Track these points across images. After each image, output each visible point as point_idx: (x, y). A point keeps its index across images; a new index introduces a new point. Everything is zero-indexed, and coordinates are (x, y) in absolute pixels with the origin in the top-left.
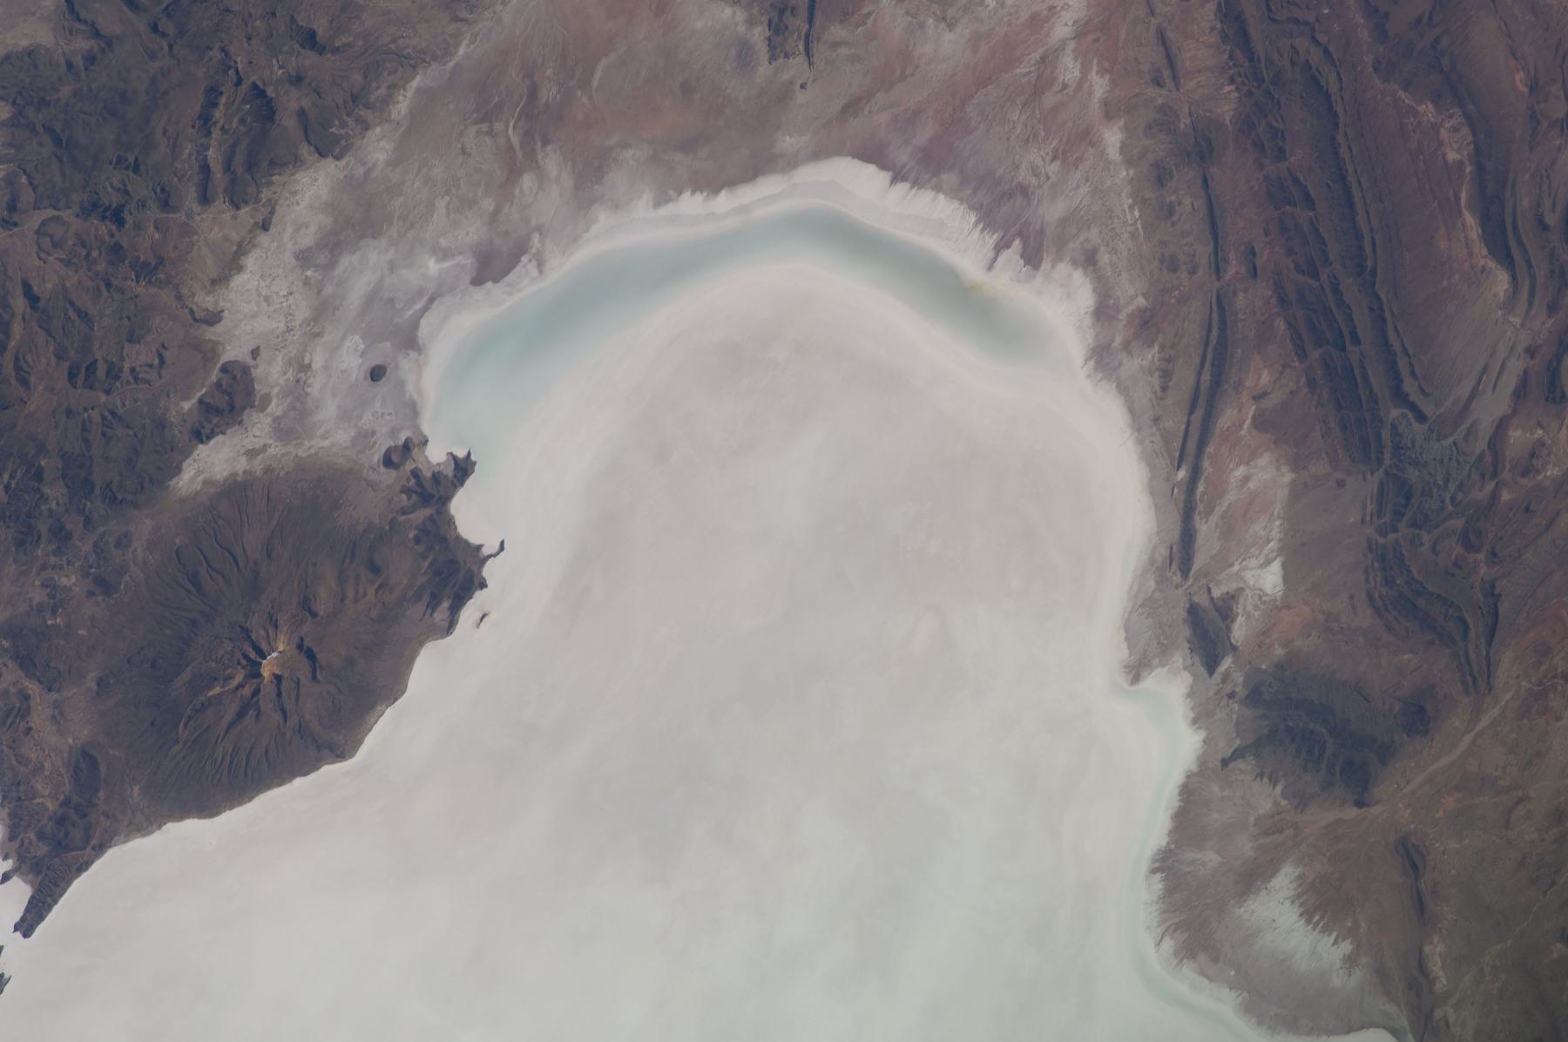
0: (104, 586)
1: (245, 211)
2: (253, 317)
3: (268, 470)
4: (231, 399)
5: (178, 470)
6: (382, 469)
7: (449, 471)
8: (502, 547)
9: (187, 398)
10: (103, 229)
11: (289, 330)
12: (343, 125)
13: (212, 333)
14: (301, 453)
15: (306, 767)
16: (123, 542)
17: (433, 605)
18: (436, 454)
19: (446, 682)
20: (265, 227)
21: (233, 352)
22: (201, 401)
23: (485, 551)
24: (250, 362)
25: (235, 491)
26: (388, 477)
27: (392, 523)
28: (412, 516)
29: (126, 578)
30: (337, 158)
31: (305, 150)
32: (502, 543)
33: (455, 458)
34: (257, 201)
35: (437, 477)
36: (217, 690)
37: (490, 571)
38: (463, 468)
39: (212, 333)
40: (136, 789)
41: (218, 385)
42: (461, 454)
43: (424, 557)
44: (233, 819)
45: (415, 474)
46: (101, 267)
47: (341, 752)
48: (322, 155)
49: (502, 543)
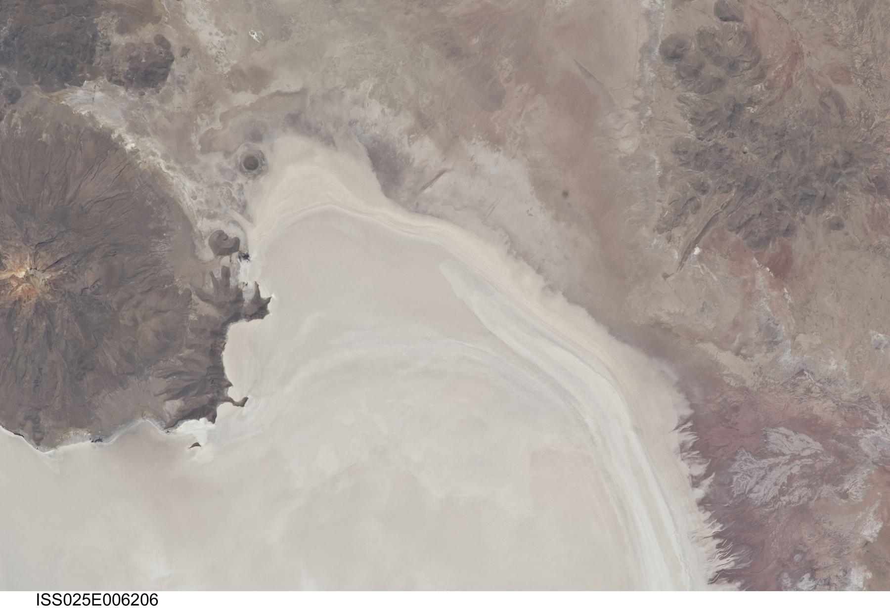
3: (134, 152)
4: (148, 73)
5: (79, 84)
7: (248, 296)
8: (243, 403)
18: (247, 275)
23: (231, 392)
25: (105, 143)
27: (187, 293)
28: (201, 302)
32: (246, 399)
33: (258, 292)
37: (223, 409)
38: (260, 309)
42: (264, 295)
45: (226, 273)
49: (246, 399)
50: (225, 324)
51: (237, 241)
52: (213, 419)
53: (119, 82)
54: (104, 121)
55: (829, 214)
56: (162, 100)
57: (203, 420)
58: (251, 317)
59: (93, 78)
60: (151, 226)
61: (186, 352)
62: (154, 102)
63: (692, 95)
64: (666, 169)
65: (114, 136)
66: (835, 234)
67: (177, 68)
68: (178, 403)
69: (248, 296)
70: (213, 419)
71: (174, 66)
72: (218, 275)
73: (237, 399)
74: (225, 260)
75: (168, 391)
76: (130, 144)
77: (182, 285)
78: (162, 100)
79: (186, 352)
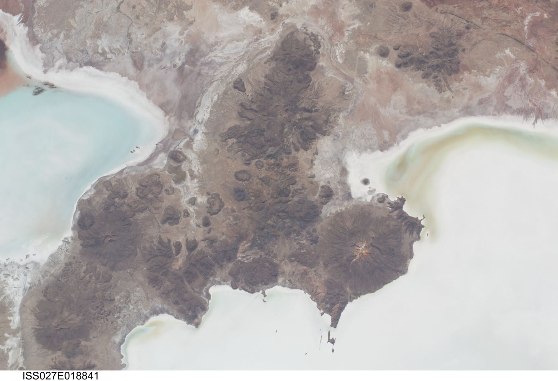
0: (315, 241)
1: (309, 151)
2: (324, 174)
3: (346, 209)
4: (328, 194)
5: (321, 212)
6: (379, 204)
8: (424, 217)
9: (315, 195)
10: (272, 161)
11: (335, 176)
12: (326, 128)
13: (315, 180)
14: (353, 203)
15: (396, 277)
16: (315, 230)
17: (411, 233)
18: (393, 198)
19: (422, 250)
20: (317, 154)
21: (322, 183)
22: (319, 196)
23: (419, 219)
24: (328, 185)
25: (339, 215)
26: (380, 205)
27: (388, 215)
29: (319, 239)
30: (329, 135)
31: (318, 135)
34: (311, 148)
35: (395, 203)
36: (354, 260)
37: (423, 223)
38: (403, 200)
39: (315, 180)
40: (348, 289)
41: (322, 191)
42: (400, 197)
43: (402, 222)
44: (379, 293)
45: (389, 203)
46: (276, 169)
47: (403, 271)
48: (324, 135)
50: (402, 210)
51: (383, 196)
52: (423, 227)
53: (327, 202)
54: (334, 211)
55: (460, 50)
56: (337, 195)
57: (423, 229)
58: (404, 204)
59: (322, 208)
60: (367, 214)
61: (403, 223)
62: (337, 197)
63: (412, 66)
64: (426, 82)
65: (339, 211)
66: (466, 52)
67: (332, 186)
68: (415, 233)
69: (399, 202)
70: (423, 227)
71: (331, 187)
72: (388, 205)
73: (422, 218)
74: (386, 202)
75: (410, 234)
76: (344, 209)
77: (385, 215)
78: (337, 195)
79: (403, 223)
